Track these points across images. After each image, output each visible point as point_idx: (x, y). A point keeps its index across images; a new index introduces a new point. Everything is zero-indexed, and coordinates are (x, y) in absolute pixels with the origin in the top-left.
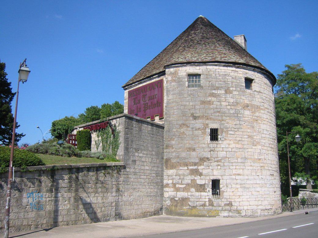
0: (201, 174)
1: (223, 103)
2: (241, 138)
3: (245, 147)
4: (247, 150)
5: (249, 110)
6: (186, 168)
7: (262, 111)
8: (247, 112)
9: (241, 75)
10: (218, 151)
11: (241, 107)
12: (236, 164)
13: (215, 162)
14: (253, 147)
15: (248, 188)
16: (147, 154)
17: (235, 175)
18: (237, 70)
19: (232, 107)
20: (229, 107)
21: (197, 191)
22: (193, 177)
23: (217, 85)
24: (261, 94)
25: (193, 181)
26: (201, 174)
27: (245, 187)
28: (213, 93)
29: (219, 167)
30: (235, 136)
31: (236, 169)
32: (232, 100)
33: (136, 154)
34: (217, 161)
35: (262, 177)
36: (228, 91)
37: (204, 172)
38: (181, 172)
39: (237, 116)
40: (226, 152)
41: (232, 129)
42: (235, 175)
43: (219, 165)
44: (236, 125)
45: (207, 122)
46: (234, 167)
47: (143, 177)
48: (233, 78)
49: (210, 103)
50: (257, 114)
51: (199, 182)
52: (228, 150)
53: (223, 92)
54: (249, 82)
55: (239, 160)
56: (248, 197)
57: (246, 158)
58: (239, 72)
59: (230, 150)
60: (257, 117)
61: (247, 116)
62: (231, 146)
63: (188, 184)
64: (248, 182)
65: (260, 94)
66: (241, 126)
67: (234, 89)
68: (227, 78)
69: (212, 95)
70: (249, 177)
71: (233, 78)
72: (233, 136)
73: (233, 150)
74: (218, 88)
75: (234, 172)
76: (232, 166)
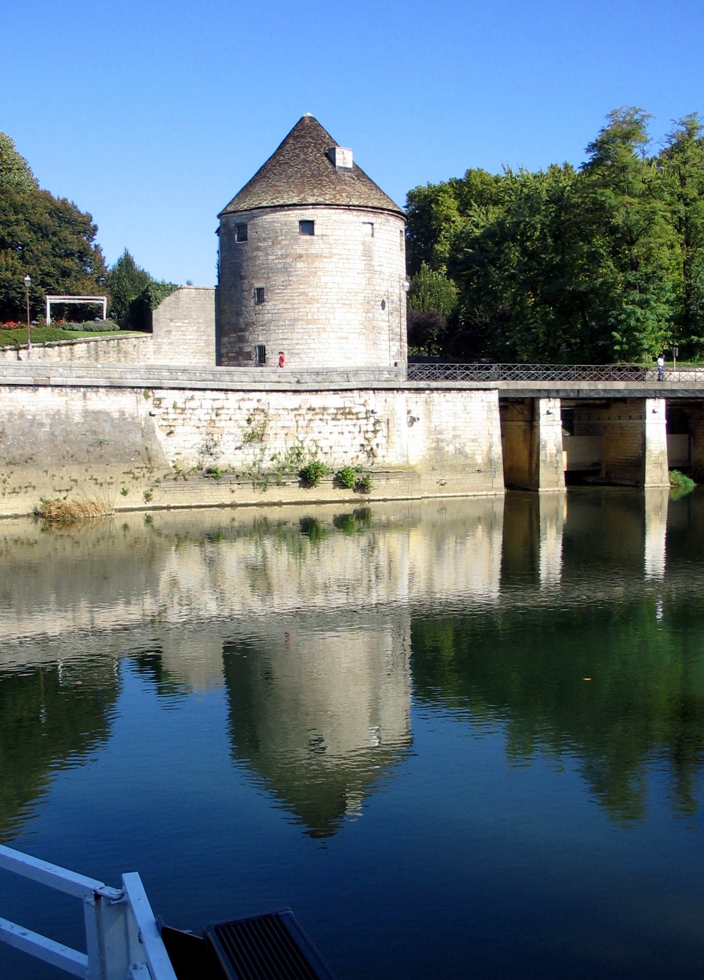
2: (291, 296)
3: (295, 306)
4: (297, 311)
5: (303, 261)
6: (235, 335)
7: (324, 260)
8: (300, 265)
9: (294, 219)
10: (263, 314)
11: (291, 259)
12: (284, 327)
13: (260, 326)
14: (307, 306)
15: (298, 354)
16: (189, 323)
17: (283, 339)
18: (288, 212)
19: (280, 261)
20: (276, 261)
23: (264, 235)
24: (327, 238)
27: (292, 353)
28: (260, 246)
29: (264, 332)
30: (283, 295)
31: (283, 333)
32: (280, 253)
33: (172, 324)
34: (262, 326)
35: (320, 340)
38: (232, 340)
39: (286, 270)
40: (272, 314)
41: (279, 287)
42: (283, 339)
43: (264, 330)
44: (283, 282)
46: (281, 331)
47: (182, 347)
48: (282, 224)
50: (317, 264)
52: (273, 312)
54: (307, 227)
55: (287, 323)
56: (298, 364)
57: (295, 320)
58: (291, 215)
59: (276, 311)
60: (316, 268)
61: (300, 269)
62: (278, 307)
63: (237, 353)
64: (297, 347)
65: (324, 237)
66: (291, 282)
67: (283, 238)
68: (276, 225)
70: (300, 342)
71: (282, 224)
72: (280, 295)
73: (279, 311)
75: (281, 336)
76: (279, 329)
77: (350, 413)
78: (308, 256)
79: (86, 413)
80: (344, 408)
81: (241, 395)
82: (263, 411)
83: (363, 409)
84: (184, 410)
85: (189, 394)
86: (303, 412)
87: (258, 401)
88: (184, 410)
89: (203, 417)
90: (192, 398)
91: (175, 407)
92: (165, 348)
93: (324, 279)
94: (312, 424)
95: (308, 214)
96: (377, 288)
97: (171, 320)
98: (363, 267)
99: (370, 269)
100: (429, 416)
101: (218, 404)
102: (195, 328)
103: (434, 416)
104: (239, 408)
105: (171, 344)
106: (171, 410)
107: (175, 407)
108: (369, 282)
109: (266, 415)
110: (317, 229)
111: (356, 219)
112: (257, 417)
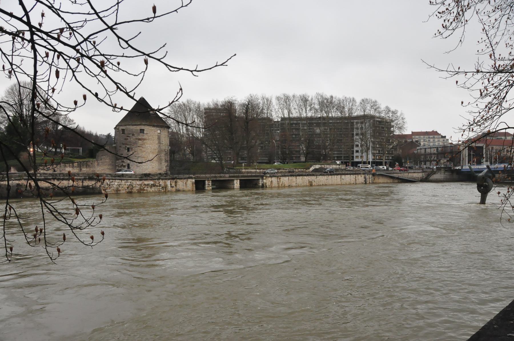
0: (124, 162)
1: (131, 139)
8: (140, 142)
21: (123, 167)
22: (122, 163)
25: (122, 164)
26: (124, 162)
32: (134, 138)
36: (133, 135)
37: (125, 161)
45: (126, 145)
49: (127, 139)
50: (145, 141)
51: (124, 165)
53: (131, 135)
54: (142, 131)
69: (128, 136)
74: (130, 134)
77: (155, 185)
78: (142, 139)
79: (83, 187)
80: (154, 184)
81: (125, 181)
82: (132, 185)
83: (158, 184)
84: (110, 185)
85: (111, 181)
86: (143, 185)
87: (130, 182)
88: (110, 185)
89: (115, 187)
90: (112, 182)
91: (107, 184)
92: (100, 164)
93: (147, 146)
94: (145, 189)
95: (142, 127)
96: (161, 148)
97: (102, 156)
98: (157, 142)
99: (159, 143)
100: (176, 186)
101: (120, 183)
102: (109, 158)
103: (178, 186)
104: (125, 184)
105: (101, 162)
106: (106, 185)
107: (107, 184)
108: (159, 146)
109: (133, 186)
110: (145, 132)
111: (156, 129)
112: (130, 187)
